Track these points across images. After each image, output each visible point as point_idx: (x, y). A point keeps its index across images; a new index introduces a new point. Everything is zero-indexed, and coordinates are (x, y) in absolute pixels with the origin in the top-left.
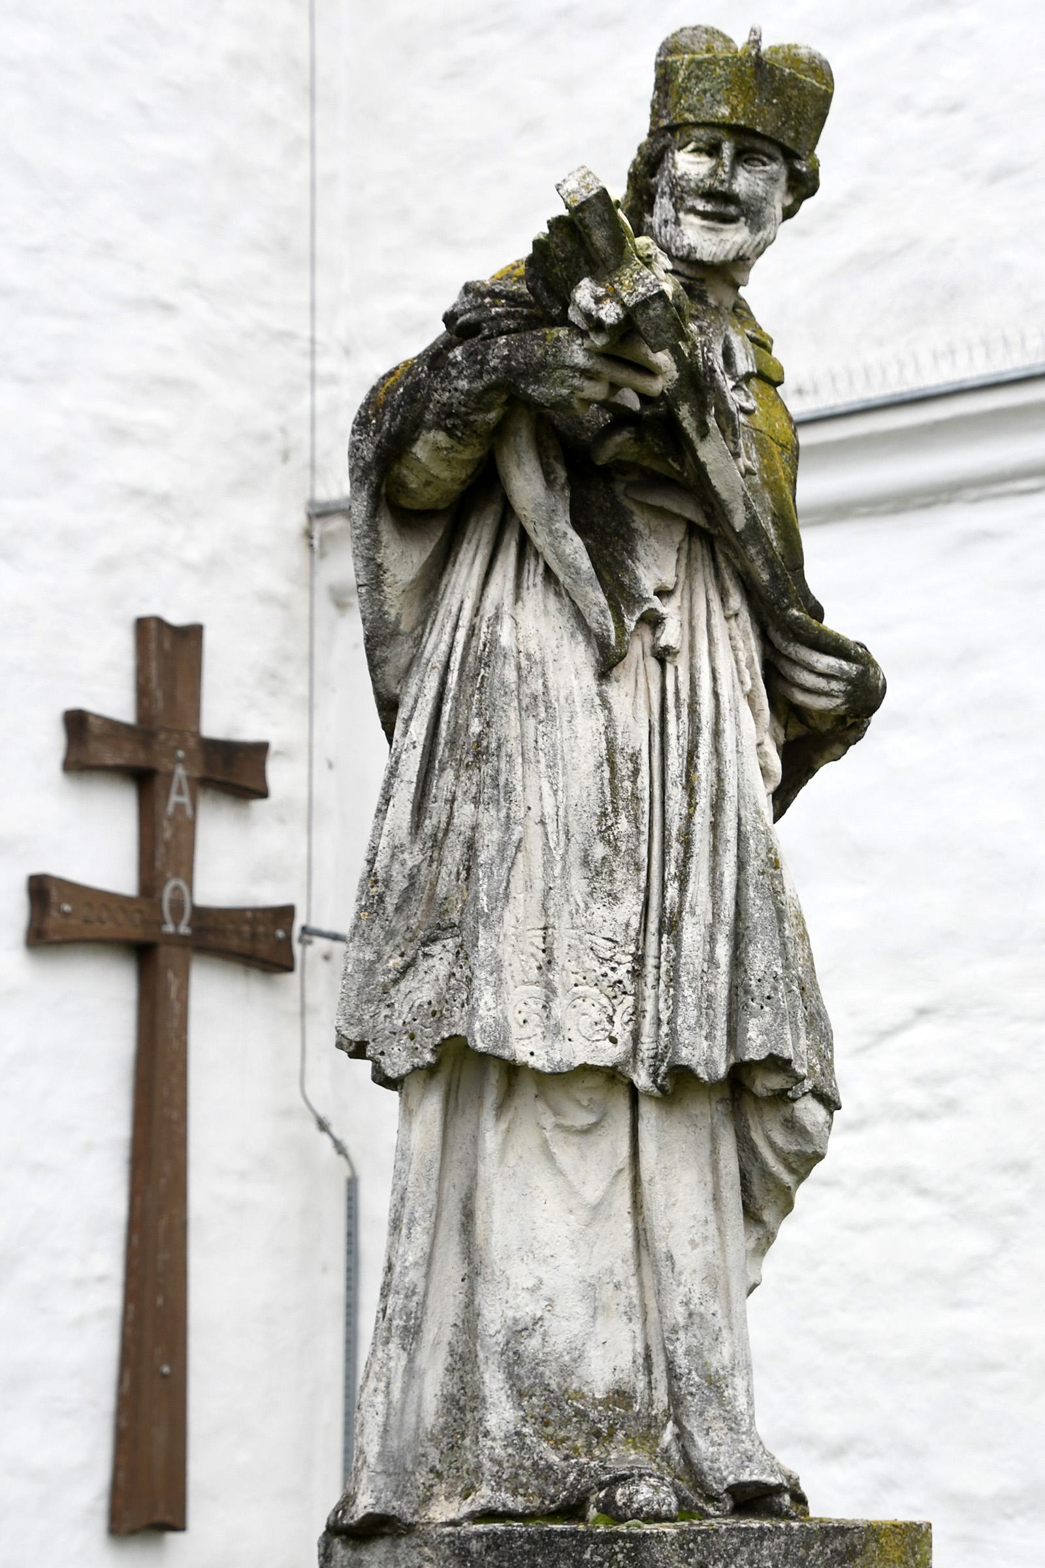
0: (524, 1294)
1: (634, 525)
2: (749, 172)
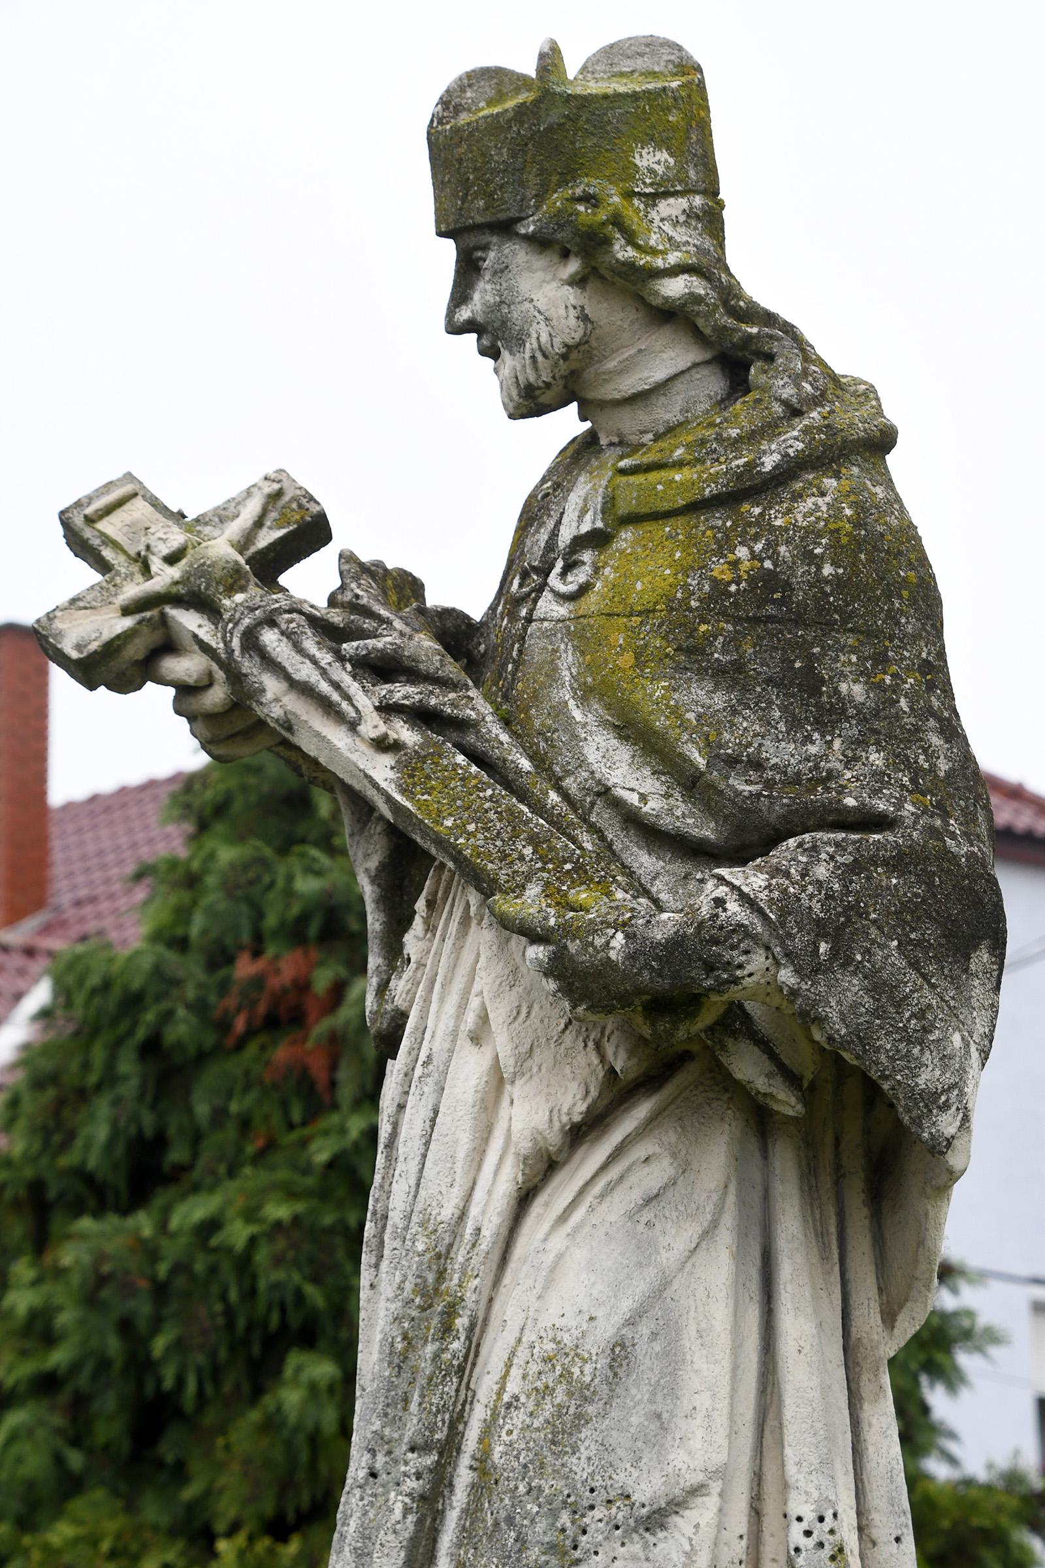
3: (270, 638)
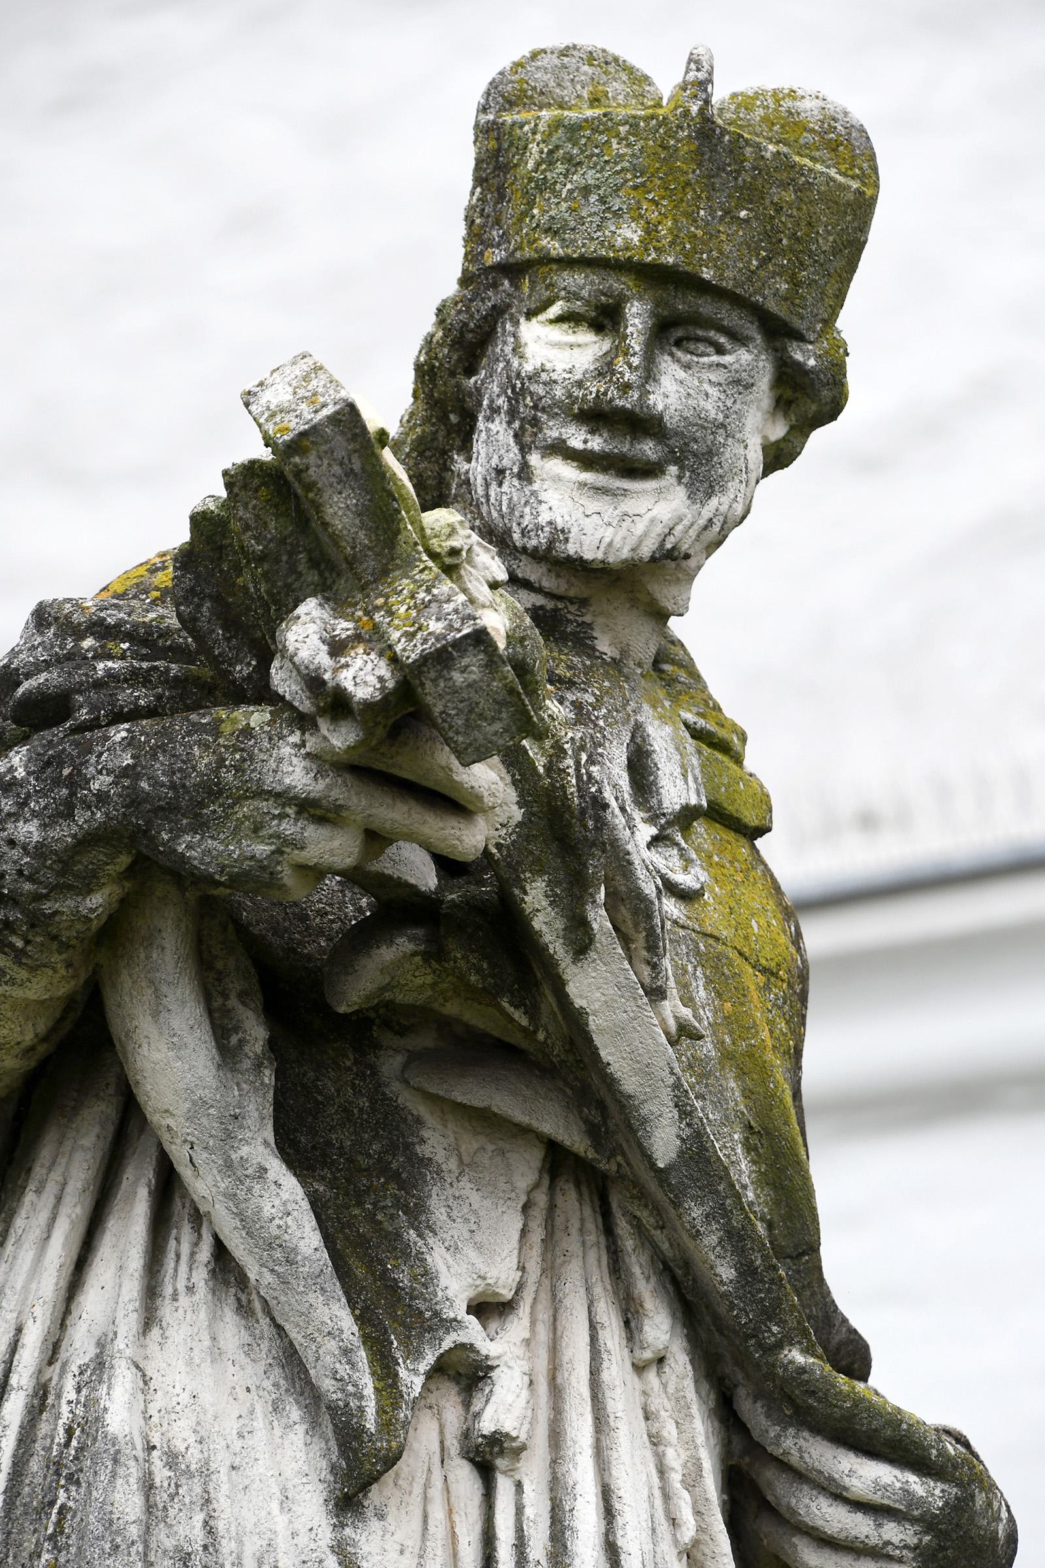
1: (424, 1150)
2: (687, 367)
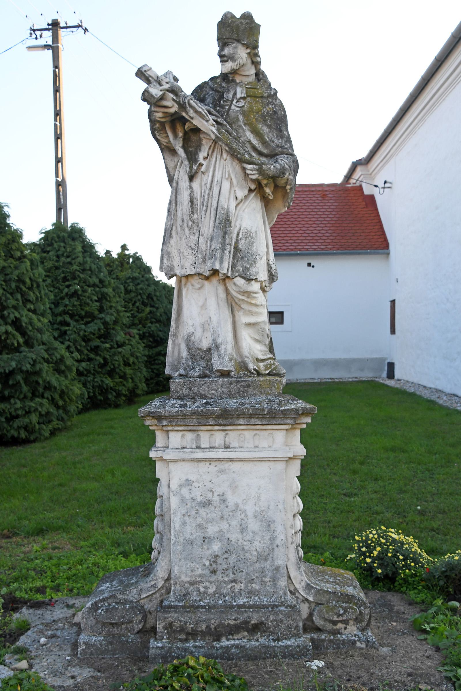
0: (191, 327)
3: (192, 102)
